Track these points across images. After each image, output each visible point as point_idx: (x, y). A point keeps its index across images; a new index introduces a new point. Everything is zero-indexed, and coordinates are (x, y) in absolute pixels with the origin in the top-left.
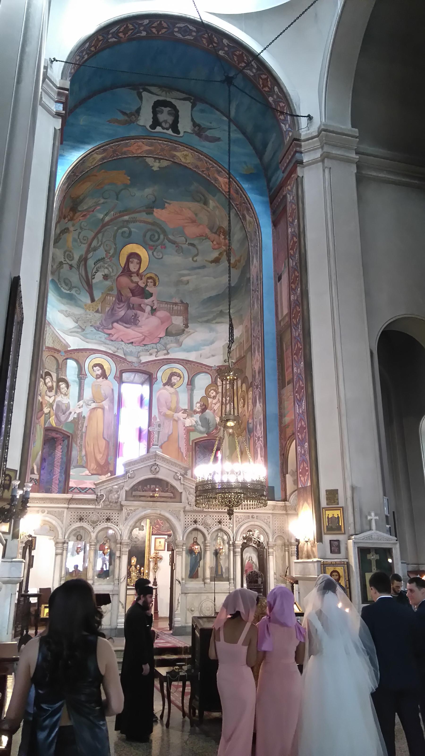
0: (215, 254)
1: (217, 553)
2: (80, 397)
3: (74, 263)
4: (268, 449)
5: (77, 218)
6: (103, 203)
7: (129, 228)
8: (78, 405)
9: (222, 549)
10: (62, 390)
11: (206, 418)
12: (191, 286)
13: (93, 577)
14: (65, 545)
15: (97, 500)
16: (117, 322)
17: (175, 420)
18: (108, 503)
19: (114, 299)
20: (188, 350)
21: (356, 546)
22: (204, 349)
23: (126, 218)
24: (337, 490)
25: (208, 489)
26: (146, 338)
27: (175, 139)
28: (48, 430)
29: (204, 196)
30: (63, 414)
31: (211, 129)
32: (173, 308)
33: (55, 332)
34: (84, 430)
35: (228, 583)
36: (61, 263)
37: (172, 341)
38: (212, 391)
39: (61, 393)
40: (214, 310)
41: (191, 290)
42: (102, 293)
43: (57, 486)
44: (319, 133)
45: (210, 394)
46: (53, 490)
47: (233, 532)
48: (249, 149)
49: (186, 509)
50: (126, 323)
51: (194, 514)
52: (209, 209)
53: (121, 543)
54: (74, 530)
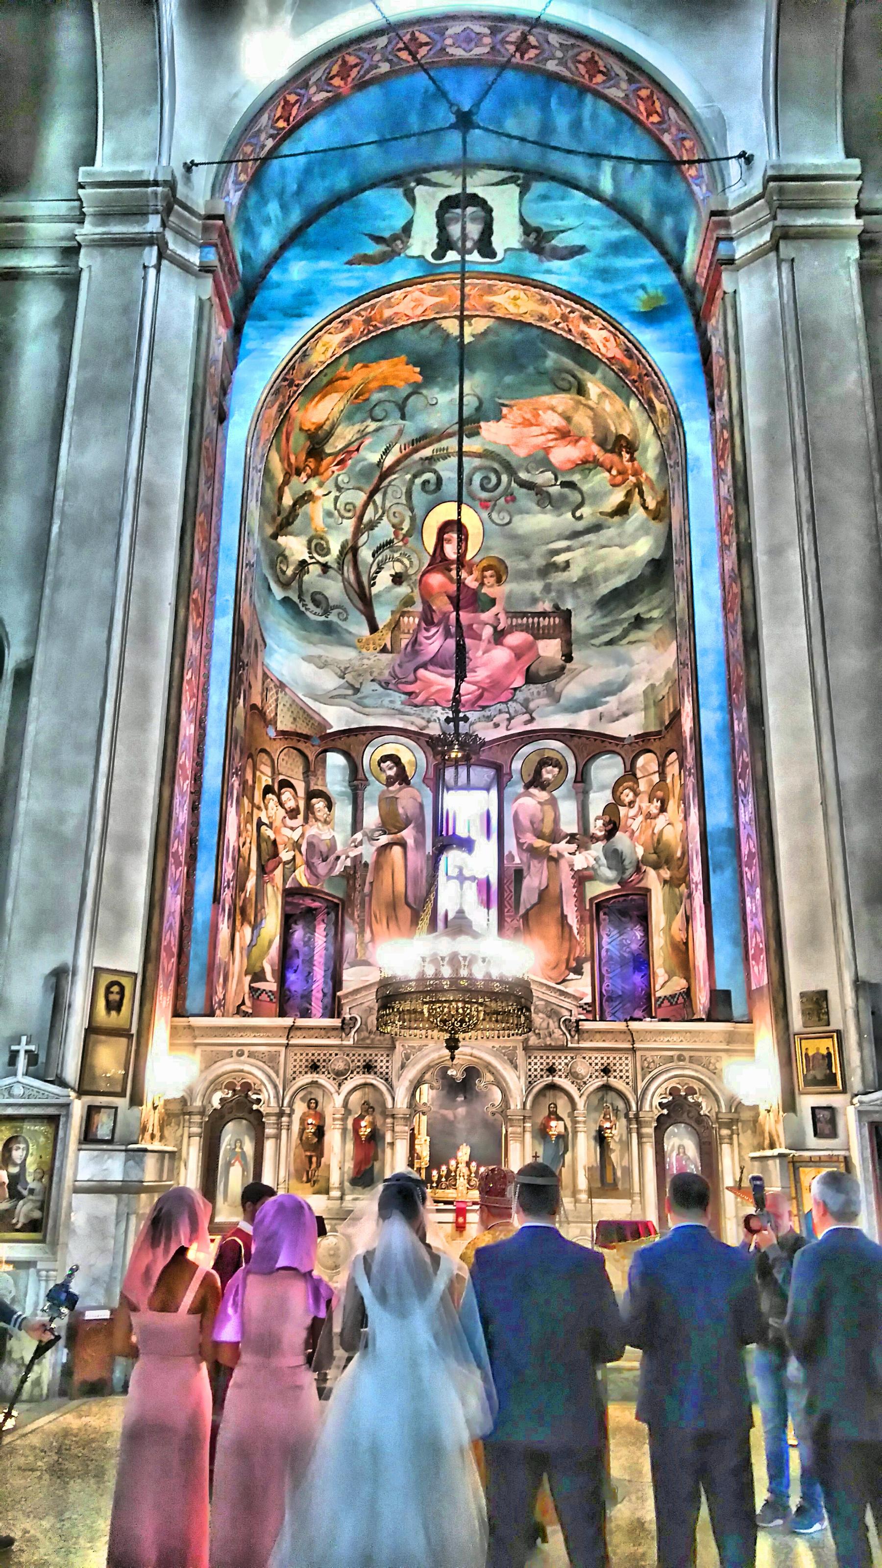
0: (617, 497)
1: (601, 1139)
2: (357, 824)
3: (331, 558)
4: (713, 908)
5: (327, 469)
6: (377, 430)
7: (435, 472)
8: (354, 841)
9: (611, 1128)
10: (318, 814)
11: (616, 851)
12: (575, 573)
13: (342, 1183)
14: (285, 1119)
15: (345, 1028)
16: (424, 666)
17: (551, 859)
18: (367, 1034)
19: (417, 620)
20: (577, 707)
21: (866, 1120)
22: (606, 703)
23: (427, 452)
24: (826, 992)
25: (410, 993)
26: (486, 694)
27: (487, 268)
28: (291, 893)
29: (574, 376)
30: (324, 861)
31: (563, 231)
32: (539, 623)
33: (297, 700)
34: (367, 889)
35: (629, 1201)
36: (303, 564)
37: (539, 693)
38: (627, 791)
39: (317, 820)
40: (624, 616)
41: (575, 580)
42: (393, 612)
43: (321, 1004)
44: (765, 187)
45: (623, 797)
46: (314, 1011)
47: (635, 1090)
48: (652, 257)
49: (531, 1043)
50: (443, 668)
51: (548, 1053)
52: (590, 403)
53: (393, 1116)
54: (302, 1088)
